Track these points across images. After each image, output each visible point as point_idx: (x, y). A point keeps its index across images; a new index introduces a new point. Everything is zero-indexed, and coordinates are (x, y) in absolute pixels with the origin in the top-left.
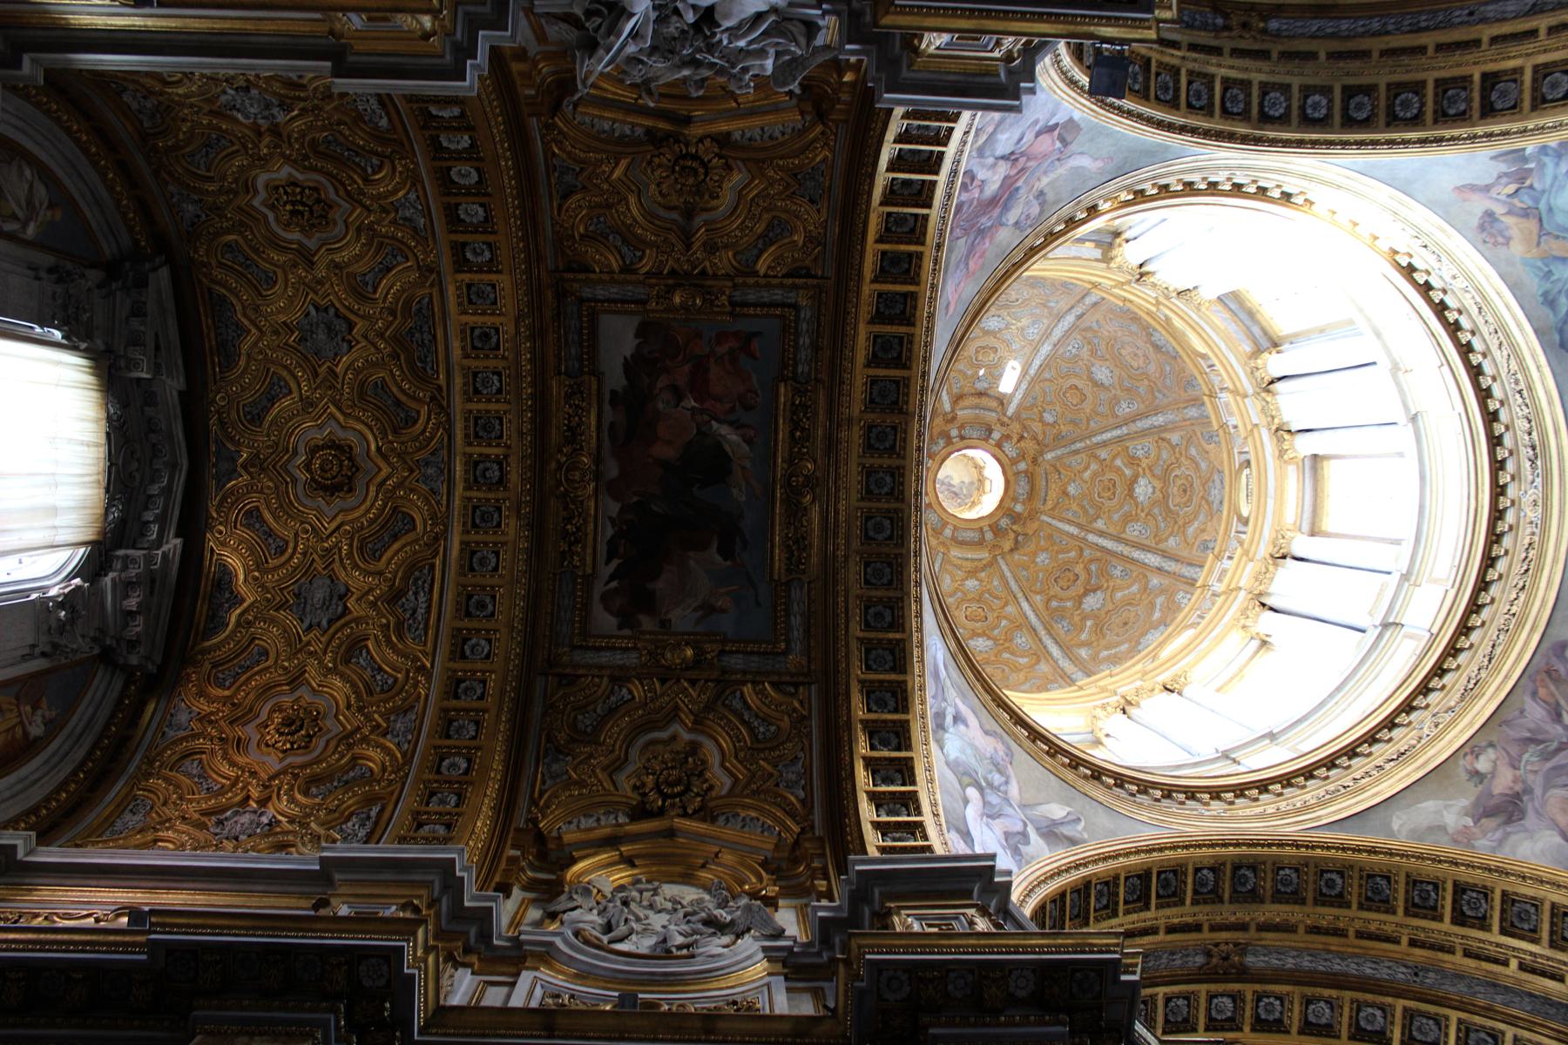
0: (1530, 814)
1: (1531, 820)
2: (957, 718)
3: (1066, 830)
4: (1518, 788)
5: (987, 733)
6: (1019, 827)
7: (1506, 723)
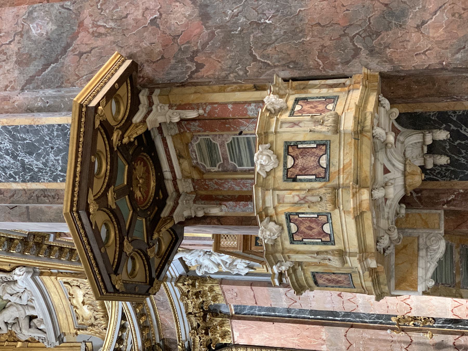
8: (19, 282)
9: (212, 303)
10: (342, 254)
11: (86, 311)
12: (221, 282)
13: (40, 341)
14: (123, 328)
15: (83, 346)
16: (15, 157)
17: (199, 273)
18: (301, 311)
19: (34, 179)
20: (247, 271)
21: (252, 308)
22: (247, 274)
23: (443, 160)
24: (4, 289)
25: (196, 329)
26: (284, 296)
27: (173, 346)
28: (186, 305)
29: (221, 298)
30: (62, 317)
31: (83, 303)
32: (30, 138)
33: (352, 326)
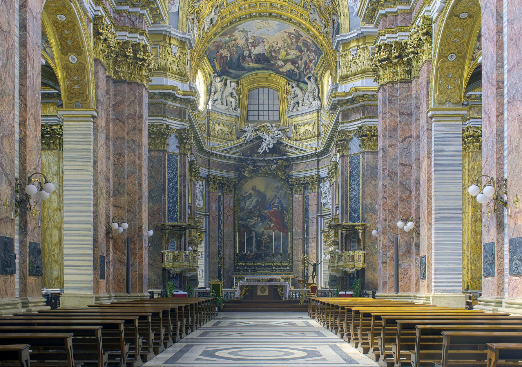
9: (309, 188)
11: (302, 130)
12: (318, 192)
13: (288, 108)
14: (297, 149)
15: (287, 128)
16: (354, 197)
17: (321, 184)
18: (308, 222)
19: (350, 200)
20: (322, 203)
21: (308, 203)
22: (321, 202)
24: (311, 92)
26: (313, 216)
27: (290, 168)
28: (308, 177)
30: (299, 118)
31: (306, 130)
32: (357, 201)
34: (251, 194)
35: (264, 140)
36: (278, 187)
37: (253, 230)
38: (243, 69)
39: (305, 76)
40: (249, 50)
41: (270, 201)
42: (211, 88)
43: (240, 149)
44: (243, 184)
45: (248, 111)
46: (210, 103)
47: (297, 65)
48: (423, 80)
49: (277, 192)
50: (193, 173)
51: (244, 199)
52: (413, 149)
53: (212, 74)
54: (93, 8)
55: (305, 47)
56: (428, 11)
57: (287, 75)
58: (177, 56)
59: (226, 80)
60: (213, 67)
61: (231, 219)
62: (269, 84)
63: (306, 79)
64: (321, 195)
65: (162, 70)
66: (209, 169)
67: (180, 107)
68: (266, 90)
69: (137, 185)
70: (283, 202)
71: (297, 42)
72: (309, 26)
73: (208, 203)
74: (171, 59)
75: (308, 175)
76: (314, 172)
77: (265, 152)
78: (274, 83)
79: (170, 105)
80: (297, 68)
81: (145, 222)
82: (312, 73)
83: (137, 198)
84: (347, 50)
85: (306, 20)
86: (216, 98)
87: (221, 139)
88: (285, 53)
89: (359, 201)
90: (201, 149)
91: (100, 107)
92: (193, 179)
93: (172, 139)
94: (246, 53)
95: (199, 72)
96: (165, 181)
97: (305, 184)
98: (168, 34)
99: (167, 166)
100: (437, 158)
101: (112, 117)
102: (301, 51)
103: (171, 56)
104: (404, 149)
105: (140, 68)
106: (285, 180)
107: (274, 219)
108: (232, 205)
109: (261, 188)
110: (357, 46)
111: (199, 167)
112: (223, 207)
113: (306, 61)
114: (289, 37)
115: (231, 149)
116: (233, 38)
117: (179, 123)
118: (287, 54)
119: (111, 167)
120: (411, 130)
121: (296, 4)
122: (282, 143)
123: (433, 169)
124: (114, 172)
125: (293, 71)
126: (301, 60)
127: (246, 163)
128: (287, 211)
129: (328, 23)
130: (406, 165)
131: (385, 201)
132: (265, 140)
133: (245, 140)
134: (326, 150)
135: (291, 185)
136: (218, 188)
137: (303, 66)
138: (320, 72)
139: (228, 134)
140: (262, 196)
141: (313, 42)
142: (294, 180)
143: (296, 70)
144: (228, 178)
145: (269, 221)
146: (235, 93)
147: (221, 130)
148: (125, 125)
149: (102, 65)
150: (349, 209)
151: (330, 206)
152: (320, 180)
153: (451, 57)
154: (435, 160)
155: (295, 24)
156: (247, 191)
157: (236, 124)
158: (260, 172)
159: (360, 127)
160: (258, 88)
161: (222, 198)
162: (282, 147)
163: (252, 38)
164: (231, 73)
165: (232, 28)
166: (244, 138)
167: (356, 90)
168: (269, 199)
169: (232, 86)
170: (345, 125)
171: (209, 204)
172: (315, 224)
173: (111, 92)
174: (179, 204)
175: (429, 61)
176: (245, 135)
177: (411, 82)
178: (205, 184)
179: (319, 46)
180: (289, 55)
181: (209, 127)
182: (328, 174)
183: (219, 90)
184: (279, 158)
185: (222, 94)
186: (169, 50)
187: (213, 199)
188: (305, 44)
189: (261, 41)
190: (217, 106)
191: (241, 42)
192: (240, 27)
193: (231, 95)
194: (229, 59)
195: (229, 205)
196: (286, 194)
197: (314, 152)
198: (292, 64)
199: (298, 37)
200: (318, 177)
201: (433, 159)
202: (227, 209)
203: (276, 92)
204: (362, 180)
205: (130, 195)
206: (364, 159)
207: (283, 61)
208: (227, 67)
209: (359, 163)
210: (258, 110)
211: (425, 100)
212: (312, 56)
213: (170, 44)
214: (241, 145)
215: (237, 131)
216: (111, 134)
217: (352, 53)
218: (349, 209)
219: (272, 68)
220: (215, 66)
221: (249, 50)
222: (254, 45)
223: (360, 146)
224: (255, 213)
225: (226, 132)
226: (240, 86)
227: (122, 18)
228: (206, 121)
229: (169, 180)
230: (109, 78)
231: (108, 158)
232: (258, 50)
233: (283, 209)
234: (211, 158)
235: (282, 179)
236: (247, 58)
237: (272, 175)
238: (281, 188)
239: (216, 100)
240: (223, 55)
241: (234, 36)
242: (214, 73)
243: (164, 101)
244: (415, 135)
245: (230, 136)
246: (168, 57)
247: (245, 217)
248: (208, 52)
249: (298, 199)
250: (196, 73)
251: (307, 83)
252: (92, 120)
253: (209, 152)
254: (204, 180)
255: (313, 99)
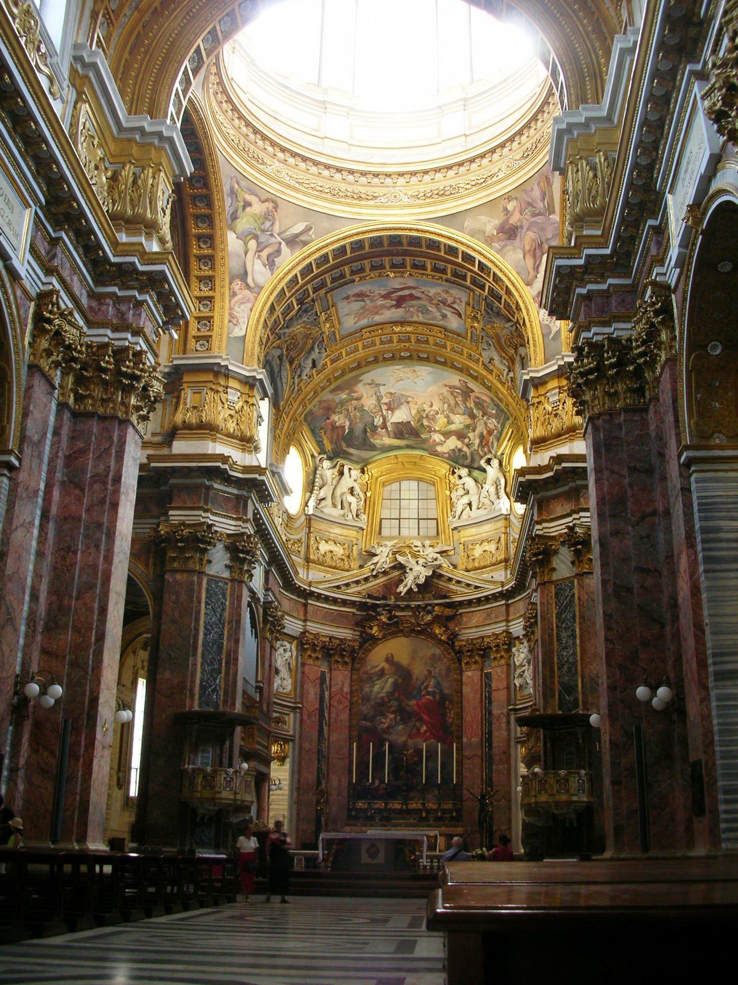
0: (518, 238)
1: (517, 242)
2: (247, 204)
3: (303, 238)
4: (519, 224)
5: (263, 202)
6: (276, 247)
7: (525, 191)
8: (498, 501)
10: (535, 796)
11: (478, 552)
12: (508, 665)
14: (468, 585)
15: (450, 548)
17: (514, 650)
18: (490, 723)
19: (559, 668)
20: (518, 685)
21: (490, 686)
23: (568, 825)
25: (471, 642)
26: (500, 712)
28: (489, 637)
29: (496, 663)
30: (473, 531)
31: (485, 551)
32: (573, 670)
33: (482, 760)
34: (383, 669)
35: (408, 571)
36: (434, 655)
37: (386, 739)
38: (373, 447)
39: (481, 457)
40: (382, 415)
41: (419, 682)
42: (314, 478)
43: (364, 587)
44: (370, 651)
45: (381, 519)
46: (312, 503)
47: (467, 440)
48: (666, 398)
49: (432, 666)
50: (268, 626)
51: (370, 679)
52: (661, 537)
53: (316, 454)
54: (39, 278)
55: (478, 409)
56: (661, 274)
57: (450, 458)
58: (237, 408)
59: (343, 466)
60: (320, 444)
61: (344, 716)
62: (419, 474)
63: (483, 463)
64: (515, 671)
65: (207, 429)
66: (305, 621)
67: (236, 495)
68: (414, 484)
69: (96, 612)
70: (445, 684)
71: (465, 401)
72: (484, 373)
73: (300, 683)
74: (225, 413)
75: (489, 633)
76: (499, 628)
77: (411, 589)
78: (428, 471)
79: (218, 490)
80: (468, 445)
81: (108, 689)
82: (493, 452)
83: (93, 639)
84: (541, 395)
85: (477, 361)
86: (322, 494)
87: (330, 567)
88: (446, 420)
89: (576, 670)
90: (289, 584)
91: (27, 450)
92: (268, 635)
93: (218, 552)
94: (378, 421)
95: (293, 450)
96: (197, 630)
97: (484, 650)
98: (223, 370)
99: (203, 600)
100: (706, 546)
101: (58, 476)
102: (472, 416)
103: (226, 406)
104: (642, 538)
105: (128, 390)
106: (448, 644)
107: (426, 717)
108: (346, 689)
109: (403, 658)
110: (560, 388)
111: (282, 617)
112: (330, 694)
113: (482, 433)
114: (452, 393)
115: (347, 585)
116: (355, 395)
117: (233, 523)
118: (450, 422)
119: (46, 571)
120: (653, 501)
121: (459, 335)
122: (441, 576)
123: (701, 568)
124: (52, 583)
125: (460, 450)
126: (474, 431)
127: (375, 611)
128: (451, 703)
129: (513, 363)
130: (647, 571)
131: (611, 646)
132: (411, 569)
133: (373, 570)
134: (520, 586)
135: (460, 652)
136: (320, 656)
137: (477, 442)
138: (507, 451)
139: (343, 560)
140: (404, 674)
141: (492, 400)
142: (464, 643)
143: (465, 449)
144: (341, 640)
145: (417, 721)
146: (357, 490)
147: (331, 552)
148: (84, 494)
149: (44, 375)
150: (557, 686)
151: (531, 691)
152: (510, 641)
153: (714, 348)
154: (704, 549)
155: (461, 370)
156: (376, 664)
157: (359, 542)
158: (401, 628)
159: (571, 529)
160: (399, 480)
161: (328, 676)
162: (442, 584)
163: (388, 395)
164: (351, 454)
165: (352, 378)
166: (373, 567)
167: (559, 459)
168: (417, 679)
169: (352, 477)
170: (545, 525)
171: (302, 686)
172: (504, 726)
173: (65, 432)
174: (223, 675)
175: (672, 361)
176: (375, 559)
177: (646, 410)
178: (297, 650)
179: (502, 406)
180: (453, 423)
181: (308, 547)
182: (525, 628)
183: (329, 481)
184: (436, 602)
185: (334, 489)
186: (224, 396)
187: (311, 677)
188: (479, 404)
189: (403, 401)
190: (324, 510)
191: (369, 403)
192: (367, 378)
193: (352, 491)
194: (347, 431)
195: (342, 689)
196: (448, 670)
197: (500, 589)
198: (458, 439)
199: (467, 393)
200: (508, 637)
201: (699, 547)
202: (337, 697)
203: (432, 488)
204: (581, 629)
205: (79, 631)
206: (583, 588)
207: (442, 434)
208: (343, 444)
209: (573, 595)
210: (399, 519)
211: (673, 432)
212: (493, 423)
213: (227, 387)
214: (366, 580)
215: (360, 554)
216: (54, 510)
217: (551, 400)
218: (557, 686)
219: (425, 446)
220: (322, 442)
221: (382, 415)
222: (391, 408)
223: (573, 563)
224: (391, 707)
225: (339, 556)
226: (366, 476)
227: (104, 308)
228: (302, 535)
229: (206, 628)
230: (62, 406)
231: (40, 554)
232: (400, 416)
233: (444, 698)
234: (309, 601)
235: (441, 640)
236: (379, 429)
237: (424, 632)
238: (439, 659)
239: (324, 499)
240: (338, 424)
241: (356, 392)
242: (320, 454)
243: (207, 483)
244: (661, 509)
245: (346, 562)
246: (220, 408)
247: (372, 713)
248: (309, 419)
249: (473, 680)
250: (286, 451)
251: (484, 471)
252: (6, 472)
253: (305, 589)
254: (295, 642)
255: (495, 497)
